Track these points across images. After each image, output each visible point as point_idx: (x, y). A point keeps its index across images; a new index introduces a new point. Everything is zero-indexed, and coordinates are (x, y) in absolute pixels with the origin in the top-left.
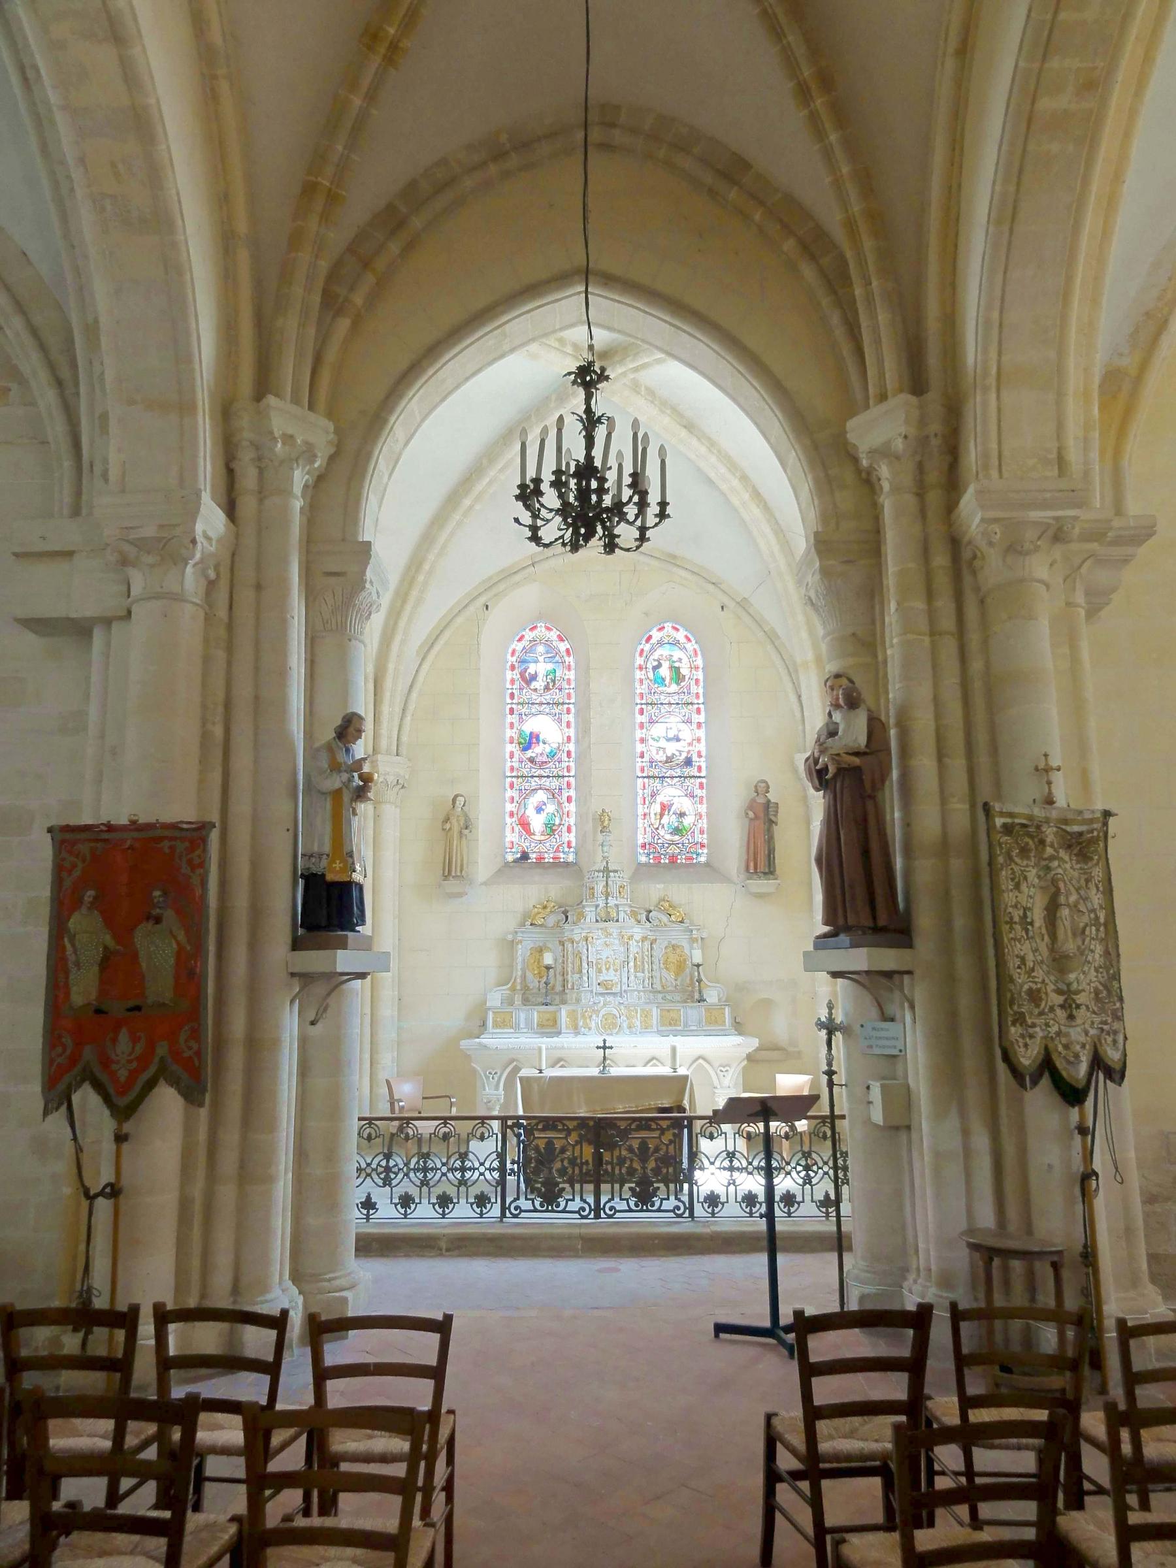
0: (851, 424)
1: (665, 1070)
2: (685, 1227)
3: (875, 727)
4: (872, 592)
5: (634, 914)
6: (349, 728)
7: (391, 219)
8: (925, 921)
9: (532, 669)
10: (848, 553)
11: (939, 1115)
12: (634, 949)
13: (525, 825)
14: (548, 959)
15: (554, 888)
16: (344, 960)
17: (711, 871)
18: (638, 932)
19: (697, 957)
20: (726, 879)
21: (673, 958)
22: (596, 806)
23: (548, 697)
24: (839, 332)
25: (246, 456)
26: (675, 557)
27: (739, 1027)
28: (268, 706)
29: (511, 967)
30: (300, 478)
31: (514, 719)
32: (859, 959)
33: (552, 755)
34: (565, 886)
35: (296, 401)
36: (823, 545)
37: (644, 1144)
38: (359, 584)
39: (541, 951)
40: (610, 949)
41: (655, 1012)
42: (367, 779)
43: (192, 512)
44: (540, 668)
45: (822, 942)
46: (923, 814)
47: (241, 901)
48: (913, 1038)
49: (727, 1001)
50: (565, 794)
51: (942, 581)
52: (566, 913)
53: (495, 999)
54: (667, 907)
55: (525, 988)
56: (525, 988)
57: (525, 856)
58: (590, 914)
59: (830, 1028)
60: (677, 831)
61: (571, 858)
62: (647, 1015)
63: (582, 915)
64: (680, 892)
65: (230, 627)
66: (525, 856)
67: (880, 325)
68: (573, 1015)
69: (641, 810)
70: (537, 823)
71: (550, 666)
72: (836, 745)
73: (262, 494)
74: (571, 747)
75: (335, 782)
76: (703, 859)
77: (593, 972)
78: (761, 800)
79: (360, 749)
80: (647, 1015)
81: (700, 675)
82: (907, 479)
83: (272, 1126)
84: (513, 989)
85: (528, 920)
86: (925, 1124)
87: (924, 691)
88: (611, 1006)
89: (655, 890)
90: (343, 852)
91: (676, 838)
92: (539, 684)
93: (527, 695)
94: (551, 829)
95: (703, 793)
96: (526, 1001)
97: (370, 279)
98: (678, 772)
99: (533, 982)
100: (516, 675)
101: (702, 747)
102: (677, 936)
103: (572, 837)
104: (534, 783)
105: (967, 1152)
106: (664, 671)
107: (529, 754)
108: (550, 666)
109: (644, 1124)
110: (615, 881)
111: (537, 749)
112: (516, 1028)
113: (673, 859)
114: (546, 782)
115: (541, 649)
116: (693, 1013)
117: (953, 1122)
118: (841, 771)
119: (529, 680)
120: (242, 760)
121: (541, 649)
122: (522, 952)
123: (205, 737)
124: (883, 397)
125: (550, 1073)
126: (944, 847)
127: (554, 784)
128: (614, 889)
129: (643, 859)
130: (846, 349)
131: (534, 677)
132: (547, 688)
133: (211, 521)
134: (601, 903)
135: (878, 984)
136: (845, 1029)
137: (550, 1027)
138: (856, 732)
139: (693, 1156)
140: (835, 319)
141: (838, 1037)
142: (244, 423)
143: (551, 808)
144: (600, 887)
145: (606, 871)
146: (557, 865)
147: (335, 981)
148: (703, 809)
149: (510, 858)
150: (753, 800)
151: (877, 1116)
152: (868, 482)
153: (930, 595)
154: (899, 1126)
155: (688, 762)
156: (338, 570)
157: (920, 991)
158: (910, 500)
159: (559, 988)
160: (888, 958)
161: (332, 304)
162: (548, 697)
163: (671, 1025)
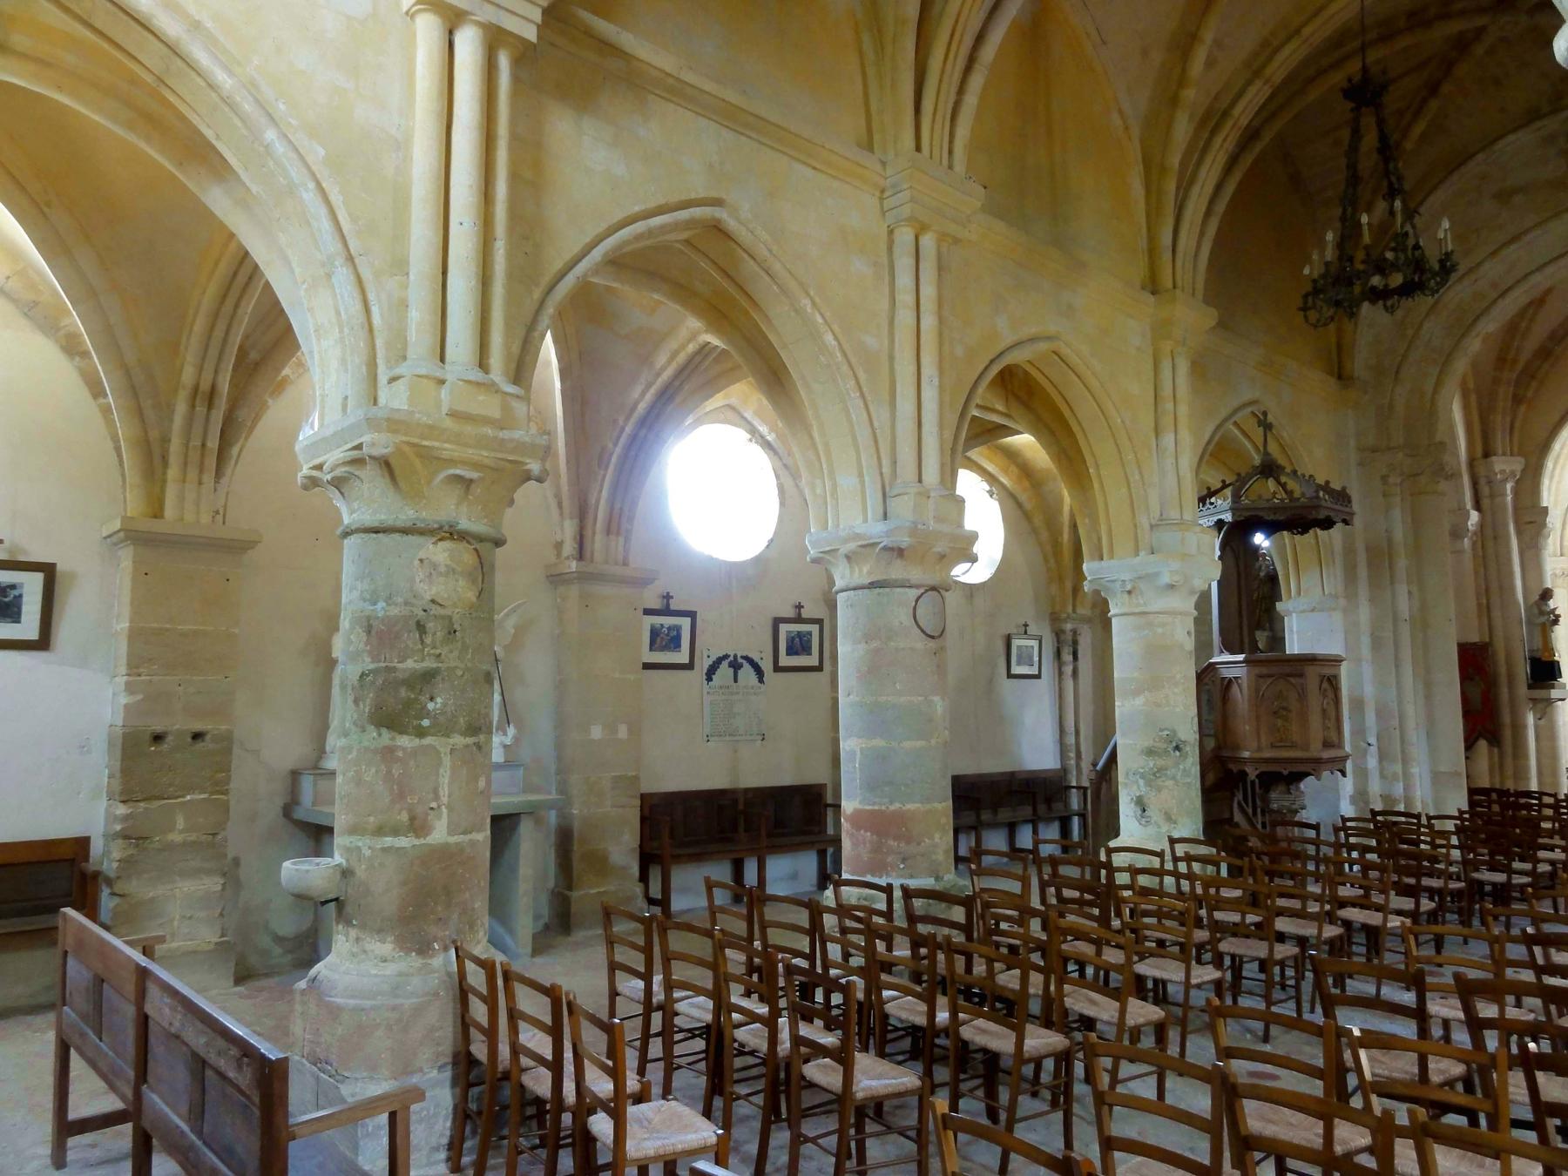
6: (1547, 595)
7: (1545, 353)
16: (1555, 693)
25: (1482, 481)
28: (1506, 588)
30: (1509, 486)
35: (1504, 454)
38: (1544, 525)
43: (1468, 517)
47: (1503, 670)
65: (1484, 557)
73: (1492, 496)
75: (1543, 619)
79: (1552, 604)
83: (1526, 757)
90: (1551, 651)
97: (1534, 384)
120: (1496, 614)
123: (1479, 605)
133: (1474, 516)
142: (1481, 471)
147: (1549, 702)
156: (1532, 519)
161: (1517, 400)
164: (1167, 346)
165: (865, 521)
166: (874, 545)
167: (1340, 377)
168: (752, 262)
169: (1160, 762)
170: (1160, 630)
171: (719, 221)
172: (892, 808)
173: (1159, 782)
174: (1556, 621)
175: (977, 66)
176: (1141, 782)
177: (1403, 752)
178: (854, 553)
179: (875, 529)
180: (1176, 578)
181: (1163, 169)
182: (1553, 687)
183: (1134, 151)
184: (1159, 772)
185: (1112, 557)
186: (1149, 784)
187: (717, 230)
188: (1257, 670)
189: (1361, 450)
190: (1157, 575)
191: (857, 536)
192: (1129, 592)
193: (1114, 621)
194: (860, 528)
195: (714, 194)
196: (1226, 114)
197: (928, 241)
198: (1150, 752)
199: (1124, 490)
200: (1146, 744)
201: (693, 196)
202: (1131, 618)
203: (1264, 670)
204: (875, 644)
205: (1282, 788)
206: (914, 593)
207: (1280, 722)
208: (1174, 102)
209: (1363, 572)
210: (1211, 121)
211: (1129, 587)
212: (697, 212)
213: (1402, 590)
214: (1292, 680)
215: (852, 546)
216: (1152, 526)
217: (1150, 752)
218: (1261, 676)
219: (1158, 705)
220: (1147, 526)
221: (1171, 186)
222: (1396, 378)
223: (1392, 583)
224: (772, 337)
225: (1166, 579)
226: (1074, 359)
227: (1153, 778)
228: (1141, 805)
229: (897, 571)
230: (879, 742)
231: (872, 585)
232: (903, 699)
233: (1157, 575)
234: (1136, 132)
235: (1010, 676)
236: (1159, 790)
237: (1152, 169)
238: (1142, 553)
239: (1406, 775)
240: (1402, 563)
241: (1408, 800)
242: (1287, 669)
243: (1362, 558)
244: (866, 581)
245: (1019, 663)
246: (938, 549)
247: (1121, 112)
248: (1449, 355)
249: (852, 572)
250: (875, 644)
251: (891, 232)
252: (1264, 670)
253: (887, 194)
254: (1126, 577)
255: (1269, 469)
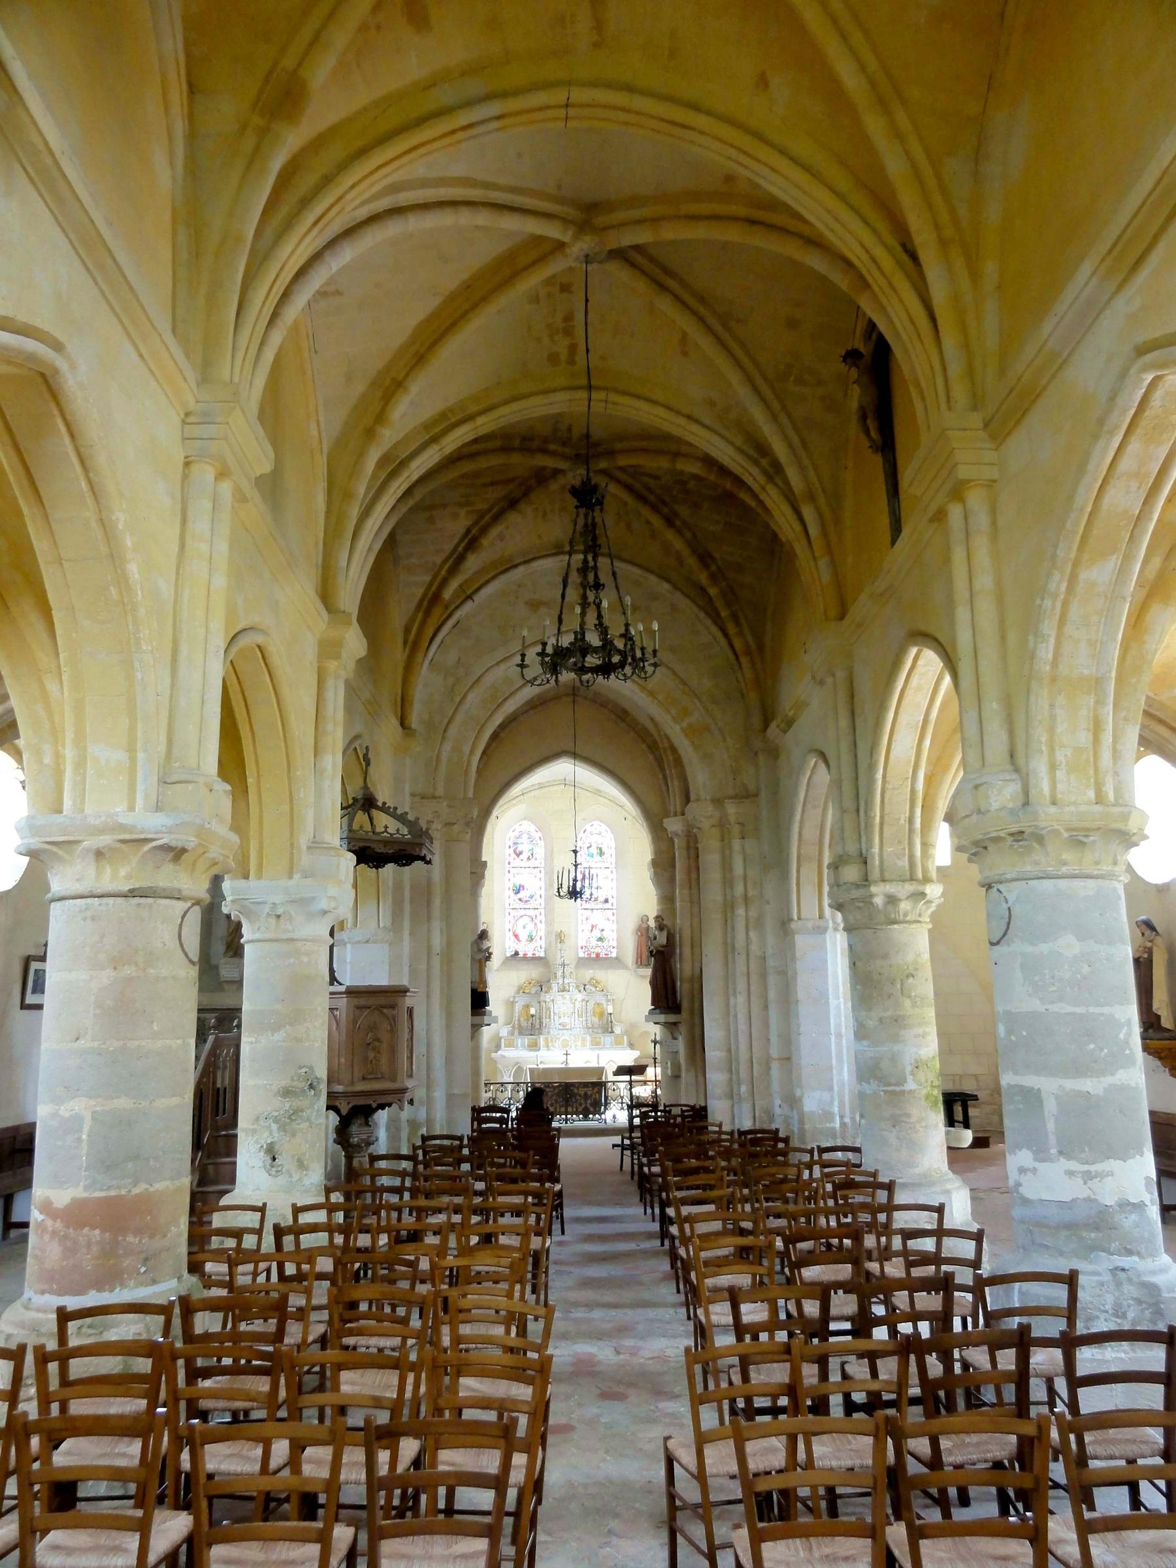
0: (665, 821)
1: (596, 1065)
2: (602, 1125)
3: (670, 938)
4: (672, 880)
5: (577, 987)
6: (483, 935)
8: (685, 1005)
9: (520, 848)
10: (663, 866)
11: (688, 1070)
12: (578, 1005)
13: (516, 936)
14: (532, 1011)
15: (534, 973)
16: (486, 1019)
17: (617, 963)
18: (580, 997)
19: (610, 1010)
20: (625, 967)
21: (598, 1010)
22: (557, 928)
23: (529, 864)
24: (662, 781)
26: (599, 791)
27: (632, 1046)
29: (512, 1015)
31: (511, 876)
32: (662, 1018)
33: (532, 897)
34: (543, 972)
36: (655, 863)
37: (586, 1094)
38: (482, 876)
39: (527, 1007)
40: (565, 1006)
41: (588, 1038)
42: (490, 954)
44: (525, 847)
45: (651, 1012)
46: (683, 968)
48: (681, 1045)
49: (627, 1032)
50: (539, 918)
51: (694, 883)
52: (542, 986)
53: (504, 1032)
54: (595, 983)
55: (520, 1026)
56: (520, 1026)
57: (517, 953)
58: (555, 987)
59: (655, 1042)
60: (600, 939)
61: (542, 955)
62: (584, 1040)
63: (550, 988)
64: (601, 974)
66: (517, 953)
67: (675, 785)
68: (546, 1041)
69: (580, 927)
70: (523, 936)
71: (531, 846)
72: (656, 943)
74: (542, 892)
76: (614, 955)
77: (556, 1018)
78: (644, 926)
79: (486, 944)
80: (584, 1040)
81: (613, 851)
82: (684, 844)
84: (513, 1027)
85: (521, 990)
86: (683, 1075)
87: (687, 924)
88: (566, 1035)
89: (588, 974)
91: (600, 943)
92: (524, 856)
93: (517, 862)
94: (531, 939)
95: (614, 918)
96: (520, 1033)
98: (600, 906)
99: (524, 1024)
100: (511, 851)
101: (614, 892)
102: (600, 998)
103: (543, 943)
104: (522, 912)
105: (697, 1082)
106: (594, 850)
107: (519, 896)
108: (531, 846)
109: (586, 1085)
110: (568, 970)
111: (521, 895)
112: (517, 1047)
113: (598, 955)
114: (528, 912)
115: (525, 837)
116: (608, 1039)
117: (692, 1074)
118: (658, 951)
119: (518, 854)
121: (525, 837)
122: (518, 1007)
124: (675, 815)
125: (541, 1066)
126: (692, 979)
127: (532, 913)
128: (567, 973)
129: (581, 955)
130: (664, 788)
131: (521, 853)
132: (529, 859)
134: (561, 982)
135: (671, 1027)
136: (661, 1043)
137: (534, 1046)
138: (662, 939)
139: (606, 1098)
140: (661, 776)
141: (658, 1046)
143: (531, 926)
144: (559, 973)
145: (563, 965)
146: (535, 959)
148: (615, 927)
149: (508, 955)
150: (640, 926)
151: (669, 1072)
152: (671, 841)
153: (690, 888)
154: (676, 1077)
155: (606, 901)
157: (683, 1028)
158: (685, 852)
159: (537, 1026)
160: (672, 1018)
162: (529, 864)
163: (596, 1044)
164: (332, 665)
165: (132, 808)
166: (146, 841)
167: (402, 724)
168: (67, 440)
169: (296, 1103)
170: (305, 959)
171: (56, 372)
172: (136, 1191)
173: (294, 1125)
174: (488, 958)
175: (279, 322)
176: (274, 1127)
177: (428, 1076)
178: (111, 849)
179: (152, 823)
180: (333, 904)
181: (348, 495)
182: (484, 1014)
183: (322, 461)
184: (293, 1115)
185: (260, 877)
186: (283, 1128)
187: (47, 383)
188: (356, 1001)
189: (413, 795)
190: (313, 898)
191: (122, 828)
192: (278, 916)
193: (247, 948)
194: (126, 819)
195: (57, 333)
196: (403, 464)
197: (226, 487)
198: (287, 1093)
199: (286, 808)
200: (283, 1083)
201: (38, 323)
202: (266, 946)
203: (362, 1001)
204: (129, 971)
205: (361, 1121)
206: (181, 906)
207: (371, 1055)
208: (370, 434)
209: (407, 906)
210: (393, 465)
211: (279, 912)
212: (30, 345)
213: (437, 925)
214: (385, 1011)
215: (106, 840)
216: (309, 848)
217: (287, 1093)
218: (358, 1007)
219: (298, 1040)
220: (304, 847)
221: (354, 512)
222: (443, 738)
223: (429, 919)
224: (40, 545)
225: (324, 904)
226: (276, 660)
227: (288, 1121)
228: (273, 1155)
229: (168, 876)
230: (123, 1103)
231: (132, 894)
232: (159, 1043)
233: (313, 898)
234: (325, 450)
235: (24, 1006)
236: (294, 1135)
237: (337, 492)
238: (297, 876)
239: (429, 1102)
240: (437, 902)
241: (429, 1121)
242: (382, 1000)
243: (407, 894)
244: (126, 888)
245: (34, 991)
246: (211, 855)
247: (318, 422)
248: (483, 726)
249: (99, 875)
250: (129, 971)
251: (187, 464)
252: (362, 1001)
253: (191, 419)
254: (278, 899)
255: (368, 803)
